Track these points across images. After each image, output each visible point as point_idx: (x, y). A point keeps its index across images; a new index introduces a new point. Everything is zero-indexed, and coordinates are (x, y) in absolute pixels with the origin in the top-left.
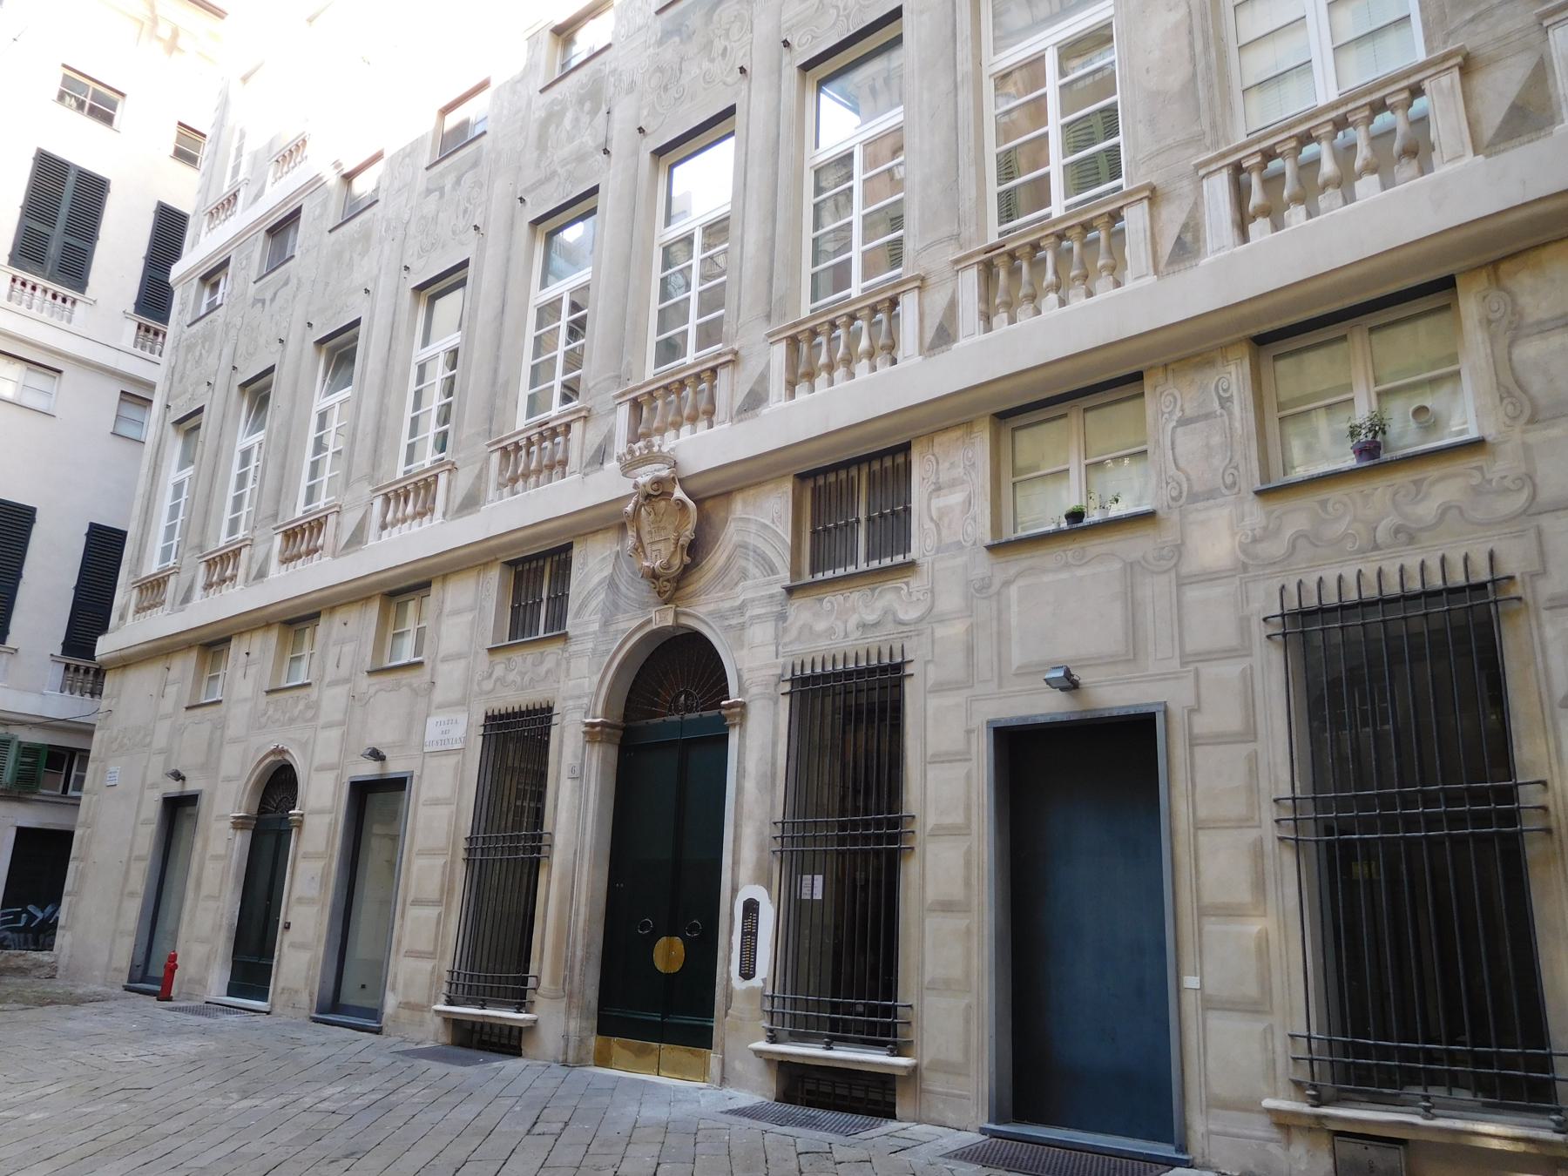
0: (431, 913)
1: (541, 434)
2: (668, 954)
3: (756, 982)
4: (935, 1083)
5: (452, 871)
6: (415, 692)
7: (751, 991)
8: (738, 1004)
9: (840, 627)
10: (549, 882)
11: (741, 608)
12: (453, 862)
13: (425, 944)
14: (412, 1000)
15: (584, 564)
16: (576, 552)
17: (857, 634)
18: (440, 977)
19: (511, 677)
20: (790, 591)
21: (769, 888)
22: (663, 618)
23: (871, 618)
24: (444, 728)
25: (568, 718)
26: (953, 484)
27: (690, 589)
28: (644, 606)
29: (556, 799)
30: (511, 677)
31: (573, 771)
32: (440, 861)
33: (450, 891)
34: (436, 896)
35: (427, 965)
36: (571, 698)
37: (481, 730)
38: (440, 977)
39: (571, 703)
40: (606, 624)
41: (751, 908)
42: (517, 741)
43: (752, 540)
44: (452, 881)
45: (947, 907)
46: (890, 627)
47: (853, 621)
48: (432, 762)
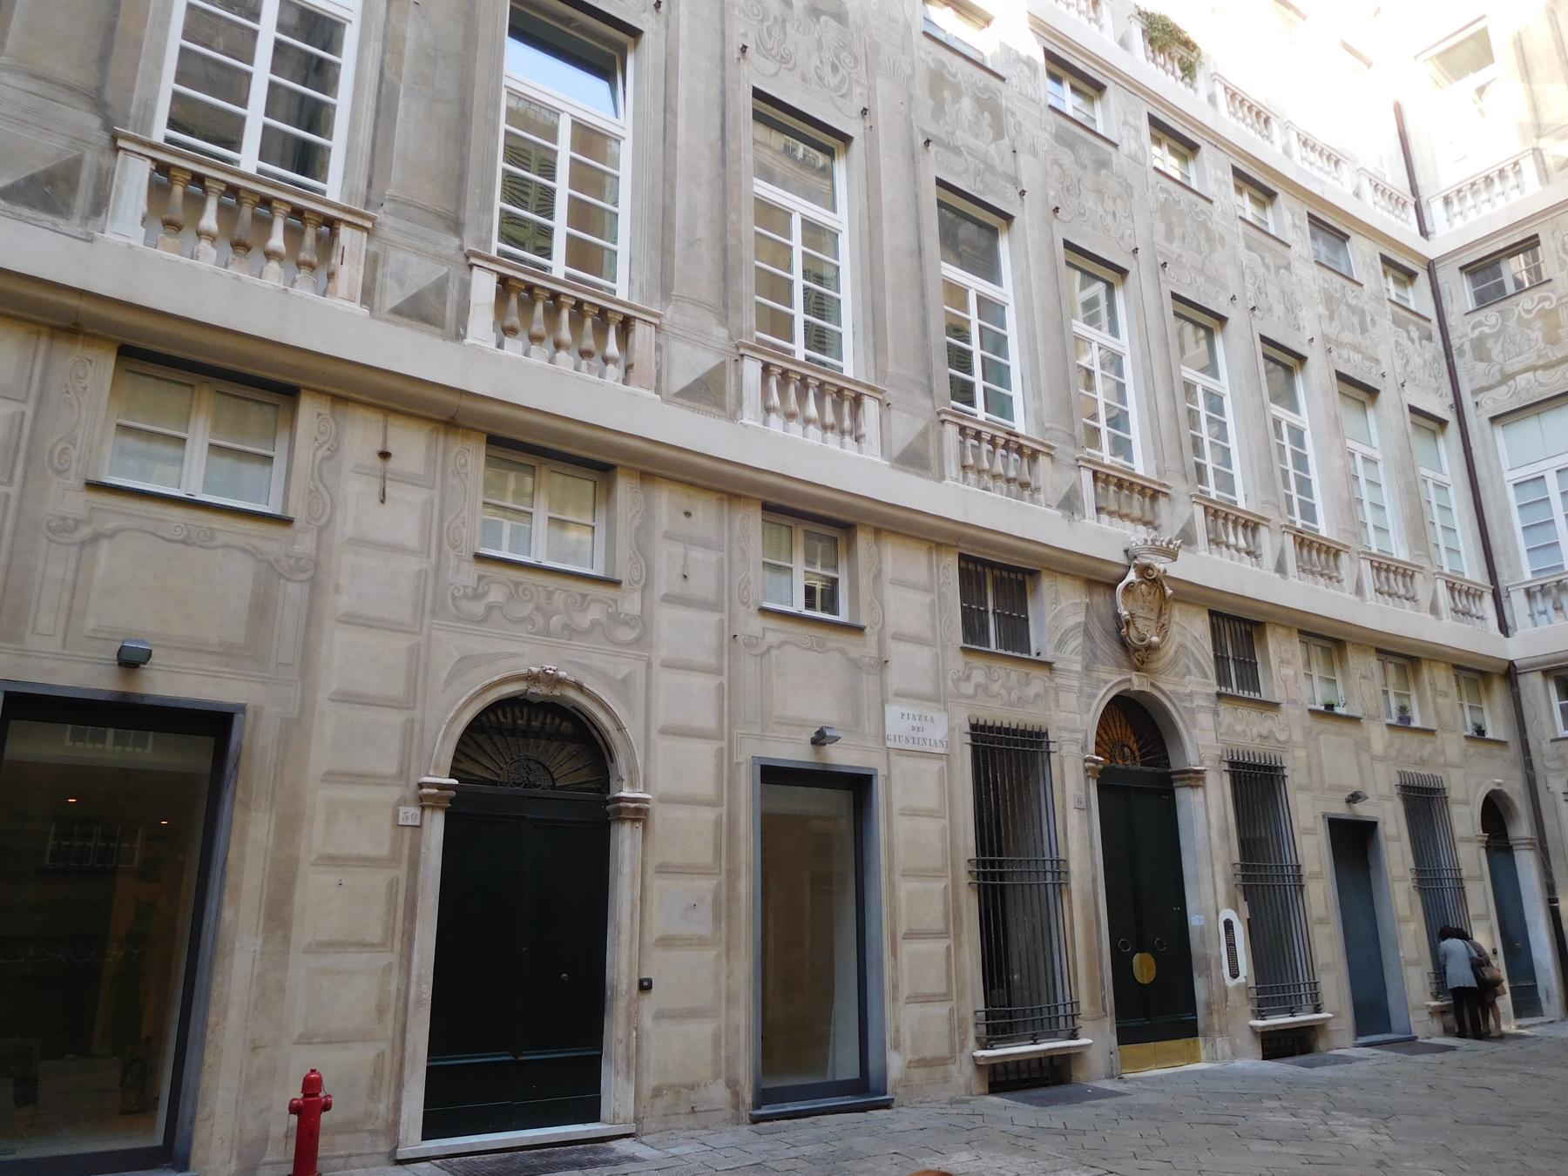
0: (938, 947)
1: (1007, 441)
2: (1144, 967)
3: (1241, 979)
4: (1332, 1026)
5: (956, 897)
6: (856, 665)
7: (1238, 986)
8: (1232, 997)
9: (1249, 732)
10: (1071, 909)
11: (1191, 695)
12: (955, 886)
13: (933, 982)
14: (928, 1053)
15: (1056, 600)
16: (1046, 582)
17: (1258, 741)
18: (962, 1021)
19: (996, 687)
20: (1219, 695)
21: (1236, 910)
22: (1138, 683)
23: (1264, 732)
24: (917, 723)
25: (1064, 751)
26: (1289, 663)
27: (1153, 666)
28: (1119, 666)
29: (1065, 827)
30: (996, 687)
31: (1080, 802)
32: (939, 886)
33: (958, 919)
34: (939, 925)
35: (942, 1009)
36: (1066, 729)
37: (968, 739)
38: (962, 1021)
39: (1065, 735)
40: (1088, 669)
41: (1228, 925)
42: (1005, 763)
43: (1189, 644)
44: (957, 910)
45: (1322, 921)
46: (1273, 742)
47: (1255, 730)
48: (902, 764)
